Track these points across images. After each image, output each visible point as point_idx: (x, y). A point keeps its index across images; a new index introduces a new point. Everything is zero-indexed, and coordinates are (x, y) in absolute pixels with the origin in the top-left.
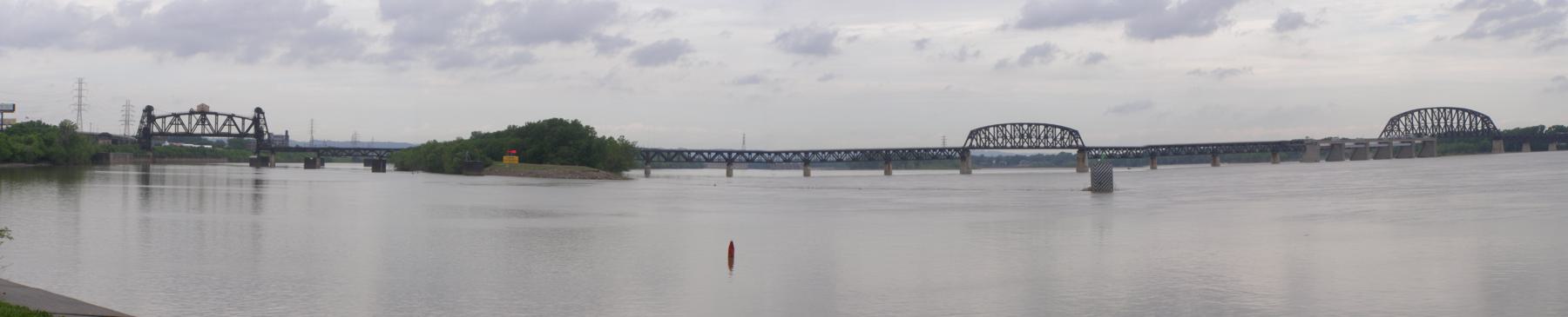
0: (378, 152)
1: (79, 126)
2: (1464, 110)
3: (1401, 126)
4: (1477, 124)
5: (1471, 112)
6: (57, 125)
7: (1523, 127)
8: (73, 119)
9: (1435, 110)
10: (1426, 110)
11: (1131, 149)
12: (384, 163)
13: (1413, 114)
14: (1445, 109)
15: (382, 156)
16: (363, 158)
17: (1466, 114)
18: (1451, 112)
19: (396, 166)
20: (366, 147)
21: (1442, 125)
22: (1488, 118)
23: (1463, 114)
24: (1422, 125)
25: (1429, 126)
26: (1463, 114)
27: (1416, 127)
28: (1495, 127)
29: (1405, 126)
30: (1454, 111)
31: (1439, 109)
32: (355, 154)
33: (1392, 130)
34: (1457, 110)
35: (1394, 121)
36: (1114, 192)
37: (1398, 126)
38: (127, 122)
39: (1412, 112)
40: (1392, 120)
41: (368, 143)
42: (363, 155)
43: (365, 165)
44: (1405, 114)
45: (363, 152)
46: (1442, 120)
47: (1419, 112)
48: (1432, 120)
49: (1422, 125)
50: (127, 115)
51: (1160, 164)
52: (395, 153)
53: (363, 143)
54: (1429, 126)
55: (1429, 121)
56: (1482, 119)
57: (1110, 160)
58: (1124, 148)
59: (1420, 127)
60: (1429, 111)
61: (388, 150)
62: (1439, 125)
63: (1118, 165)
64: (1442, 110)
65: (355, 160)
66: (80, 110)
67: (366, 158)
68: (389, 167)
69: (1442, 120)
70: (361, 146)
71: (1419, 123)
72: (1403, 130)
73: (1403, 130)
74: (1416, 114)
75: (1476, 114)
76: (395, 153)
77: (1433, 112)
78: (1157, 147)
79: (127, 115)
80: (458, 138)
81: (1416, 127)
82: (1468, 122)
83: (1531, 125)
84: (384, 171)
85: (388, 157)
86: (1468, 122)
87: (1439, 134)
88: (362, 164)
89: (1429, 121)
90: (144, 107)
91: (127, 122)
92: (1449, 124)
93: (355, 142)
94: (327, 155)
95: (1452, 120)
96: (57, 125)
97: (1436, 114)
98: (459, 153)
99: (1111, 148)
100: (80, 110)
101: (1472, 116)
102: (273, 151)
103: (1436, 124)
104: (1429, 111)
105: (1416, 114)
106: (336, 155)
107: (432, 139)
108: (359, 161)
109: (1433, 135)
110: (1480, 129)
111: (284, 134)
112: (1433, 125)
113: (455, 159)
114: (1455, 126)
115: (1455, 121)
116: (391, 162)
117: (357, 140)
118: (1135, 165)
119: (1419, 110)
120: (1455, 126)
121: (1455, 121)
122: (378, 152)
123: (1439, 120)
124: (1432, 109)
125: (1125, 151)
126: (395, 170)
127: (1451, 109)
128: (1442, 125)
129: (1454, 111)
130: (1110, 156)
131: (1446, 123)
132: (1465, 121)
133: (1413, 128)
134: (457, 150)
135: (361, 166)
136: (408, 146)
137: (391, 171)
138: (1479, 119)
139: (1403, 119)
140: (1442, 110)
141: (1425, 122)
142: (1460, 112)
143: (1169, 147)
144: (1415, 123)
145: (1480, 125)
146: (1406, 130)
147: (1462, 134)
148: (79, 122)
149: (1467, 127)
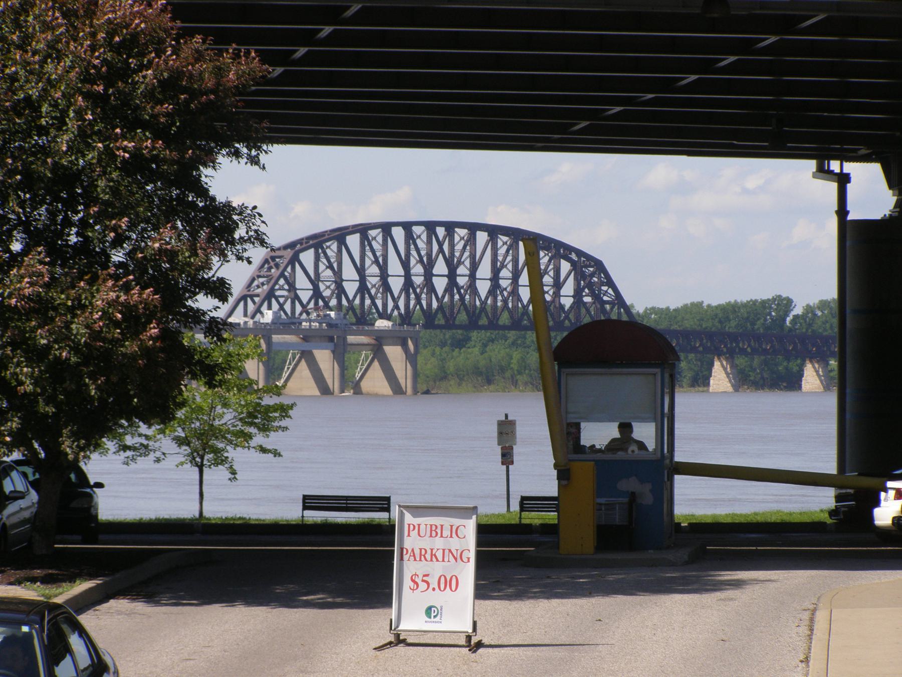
3: (302, 282)
4: (558, 285)
7: (714, 303)
9: (418, 230)
10: (386, 228)
13: (342, 242)
14: (450, 227)
18: (471, 240)
21: (441, 284)
22: (599, 266)
24: (373, 281)
25: (396, 284)
26: (513, 247)
27: (351, 288)
28: (619, 299)
29: (315, 282)
30: (482, 237)
31: (431, 226)
33: (270, 295)
39: (340, 235)
44: (317, 242)
46: (440, 267)
47: (365, 239)
48: (406, 265)
49: (373, 281)
54: (396, 284)
55: (395, 267)
59: (363, 289)
60: (398, 233)
69: (440, 267)
71: (361, 271)
72: (305, 296)
73: (305, 296)
74: (353, 241)
77: (410, 237)
81: (351, 288)
83: (743, 296)
89: (395, 267)
92: (462, 281)
95: (474, 267)
103: (418, 280)
104: (398, 233)
105: (353, 241)
112: (408, 284)
114: (483, 287)
115: (485, 270)
119: (363, 230)
120: (483, 287)
121: (485, 270)
124: (407, 226)
127: (473, 228)
128: (441, 284)
129: (482, 237)
131: (452, 276)
133: (340, 291)
138: (565, 266)
139: (307, 257)
140: (441, 231)
142: (503, 239)
144: (349, 272)
145: (568, 289)
146: (317, 294)
147: (505, 319)
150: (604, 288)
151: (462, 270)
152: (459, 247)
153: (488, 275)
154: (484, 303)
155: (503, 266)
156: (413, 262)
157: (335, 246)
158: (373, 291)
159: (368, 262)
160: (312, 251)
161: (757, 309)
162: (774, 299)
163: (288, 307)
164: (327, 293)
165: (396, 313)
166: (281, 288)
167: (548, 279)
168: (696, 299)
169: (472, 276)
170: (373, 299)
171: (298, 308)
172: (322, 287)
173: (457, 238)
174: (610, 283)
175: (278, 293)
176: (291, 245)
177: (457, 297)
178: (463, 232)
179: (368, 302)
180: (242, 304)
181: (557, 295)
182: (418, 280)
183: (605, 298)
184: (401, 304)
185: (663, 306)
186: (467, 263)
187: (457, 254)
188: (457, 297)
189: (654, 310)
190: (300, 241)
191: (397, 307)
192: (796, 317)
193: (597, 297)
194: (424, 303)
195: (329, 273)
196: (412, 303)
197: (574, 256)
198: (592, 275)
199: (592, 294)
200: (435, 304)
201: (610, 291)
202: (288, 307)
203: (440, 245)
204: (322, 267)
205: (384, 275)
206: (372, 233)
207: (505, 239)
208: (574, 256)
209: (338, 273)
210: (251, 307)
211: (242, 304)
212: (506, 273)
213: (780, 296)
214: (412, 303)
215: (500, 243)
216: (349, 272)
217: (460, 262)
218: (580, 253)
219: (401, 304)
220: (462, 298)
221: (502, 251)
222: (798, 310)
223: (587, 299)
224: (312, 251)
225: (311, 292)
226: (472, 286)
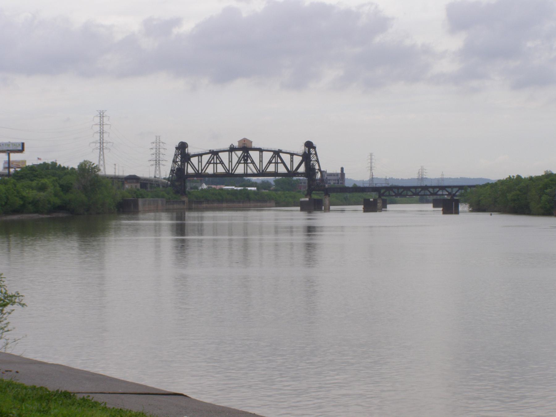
0: (449, 190)
1: (102, 168)
6: (76, 167)
8: (94, 159)
12: (457, 203)
15: (454, 195)
16: (431, 198)
19: (470, 206)
20: (434, 184)
32: (422, 193)
38: (158, 163)
41: (438, 180)
42: (432, 194)
43: (434, 207)
45: (431, 190)
50: (158, 154)
52: (469, 190)
53: (431, 180)
61: (461, 187)
65: (423, 200)
66: (101, 149)
67: (435, 197)
68: (463, 207)
70: (429, 184)
76: (469, 190)
79: (158, 154)
80: (546, 172)
84: (457, 212)
85: (461, 195)
88: (431, 205)
90: (177, 144)
91: (158, 163)
93: (422, 179)
94: (390, 195)
96: (76, 167)
98: (548, 191)
100: (101, 149)
102: (327, 191)
106: (400, 195)
107: (514, 174)
108: (427, 202)
111: (339, 171)
113: (544, 198)
116: (465, 202)
117: (424, 177)
122: (449, 190)
126: (471, 211)
134: (546, 186)
135: (429, 207)
136: (484, 183)
137: (464, 212)
148: (102, 162)
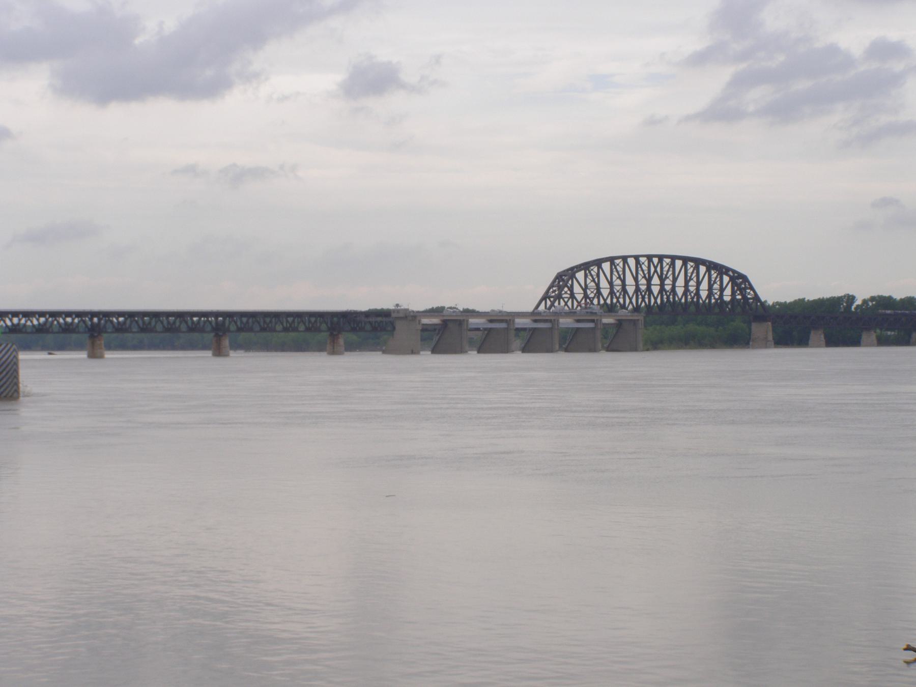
2: (698, 262)
3: (577, 289)
4: (722, 290)
5: (712, 266)
7: (811, 299)
9: (642, 259)
10: (625, 259)
11: (54, 314)
13: (600, 267)
14: (661, 258)
17: (703, 269)
18: (673, 264)
21: (656, 290)
22: (745, 278)
23: (697, 268)
24: (618, 288)
25: (631, 290)
26: (697, 268)
27: (605, 292)
28: (756, 297)
29: (585, 289)
30: (679, 263)
31: (650, 258)
33: (559, 297)
34: (685, 260)
35: (564, 278)
36: (21, 398)
37: (571, 289)
39: (598, 263)
40: (559, 277)
44: (586, 266)
46: (656, 280)
47: (612, 263)
48: (636, 279)
49: (618, 288)
51: (109, 347)
54: (631, 290)
55: (630, 280)
56: (732, 279)
57: (13, 336)
58: (42, 314)
59: (612, 293)
62: (649, 289)
63: (27, 347)
64: (655, 260)
69: (656, 280)
71: (611, 283)
72: (579, 297)
73: (579, 297)
74: (606, 266)
75: (722, 270)
78: (107, 315)
81: (605, 292)
82: (704, 285)
83: (827, 295)
86: (704, 285)
87: (648, 307)
89: (630, 280)
92: (668, 288)
95: (675, 280)
97: (645, 268)
99: (15, 314)
101: (714, 274)
103: (643, 288)
104: (632, 262)
105: (606, 266)
109: (637, 309)
110: (727, 298)
112: (637, 290)
114: (680, 291)
115: (681, 282)
118: (62, 347)
119: (612, 260)
120: (680, 291)
121: (681, 282)
123: (649, 280)
124: (637, 258)
125: (42, 320)
127: (674, 258)
128: (656, 290)
129: (679, 263)
130: (14, 329)
131: (662, 285)
132: (699, 283)
133: (599, 293)
138: (726, 279)
139: (580, 275)
140: (655, 260)
141: (623, 281)
143: (130, 315)
144: (604, 284)
145: (728, 292)
146: (586, 296)
149: (704, 294)
150: (748, 291)
151: (668, 282)
152: (666, 269)
153: (707, 288)
154: (704, 302)
155: (691, 279)
156: (640, 277)
157: (596, 269)
158: (618, 294)
159: (614, 278)
160: (583, 271)
161: (834, 302)
162: (845, 296)
163: (570, 303)
164: (592, 295)
165: (631, 307)
166: (566, 293)
167: (716, 286)
168: (801, 297)
169: (698, 289)
170: (618, 298)
171: (575, 303)
172: (589, 292)
173: (665, 264)
174: (752, 288)
175: (564, 296)
176: (572, 269)
177: (665, 297)
178: (668, 260)
179: (615, 300)
180: (544, 302)
181: (721, 296)
182: (643, 288)
183: (749, 296)
184: (634, 301)
185: (783, 301)
186: (671, 278)
187: (665, 273)
188: (665, 297)
189: (777, 303)
190: (576, 267)
191: (631, 302)
192: (858, 306)
193: (744, 297)
194: (647, 300)
195: (593, 284)
196: (640, 300)
197: (731, 273)
198: (741, 283)
199: (741, 294)
200: (653, 301)
201: (752, 292)
202: (570, 303)
203: (656, 268)
204: (588, 281)
205: (624, 285)
206: (617, 261)
207: (692, 264)
208: (731, 273)
209: (598, 285)
210: (549, 303)
211: (544, 302)
212: (692, 283)
213: (848, 294)
214: (640, 300)
215: (689, 266)
216: (604, 284)
217: (667, 277)
218: (734, 271)
219: (634, 301)
220: (668, 298)
221: (690, 271)
222: (858, 302)
223: (739, 297)
224: (583, 271)
225: (583, 295)
226: (673, 290)
